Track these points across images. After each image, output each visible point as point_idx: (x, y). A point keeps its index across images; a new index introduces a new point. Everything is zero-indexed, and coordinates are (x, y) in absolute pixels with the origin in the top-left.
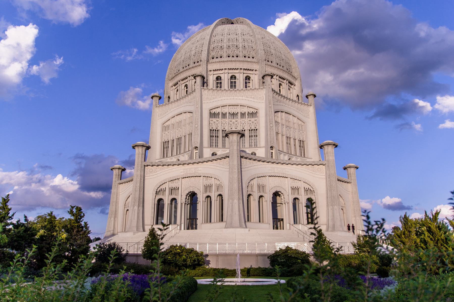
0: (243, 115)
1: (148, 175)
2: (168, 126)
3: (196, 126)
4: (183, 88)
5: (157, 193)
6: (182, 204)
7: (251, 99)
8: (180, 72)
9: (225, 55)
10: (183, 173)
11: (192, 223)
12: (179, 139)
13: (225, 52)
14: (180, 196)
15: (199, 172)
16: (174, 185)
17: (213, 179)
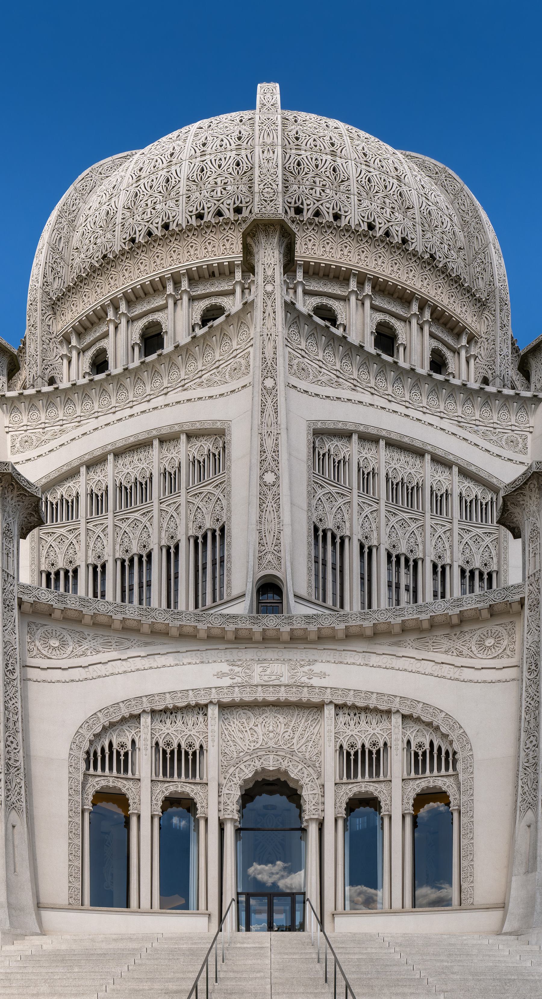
14: (213, 789)
15: (316, 682)
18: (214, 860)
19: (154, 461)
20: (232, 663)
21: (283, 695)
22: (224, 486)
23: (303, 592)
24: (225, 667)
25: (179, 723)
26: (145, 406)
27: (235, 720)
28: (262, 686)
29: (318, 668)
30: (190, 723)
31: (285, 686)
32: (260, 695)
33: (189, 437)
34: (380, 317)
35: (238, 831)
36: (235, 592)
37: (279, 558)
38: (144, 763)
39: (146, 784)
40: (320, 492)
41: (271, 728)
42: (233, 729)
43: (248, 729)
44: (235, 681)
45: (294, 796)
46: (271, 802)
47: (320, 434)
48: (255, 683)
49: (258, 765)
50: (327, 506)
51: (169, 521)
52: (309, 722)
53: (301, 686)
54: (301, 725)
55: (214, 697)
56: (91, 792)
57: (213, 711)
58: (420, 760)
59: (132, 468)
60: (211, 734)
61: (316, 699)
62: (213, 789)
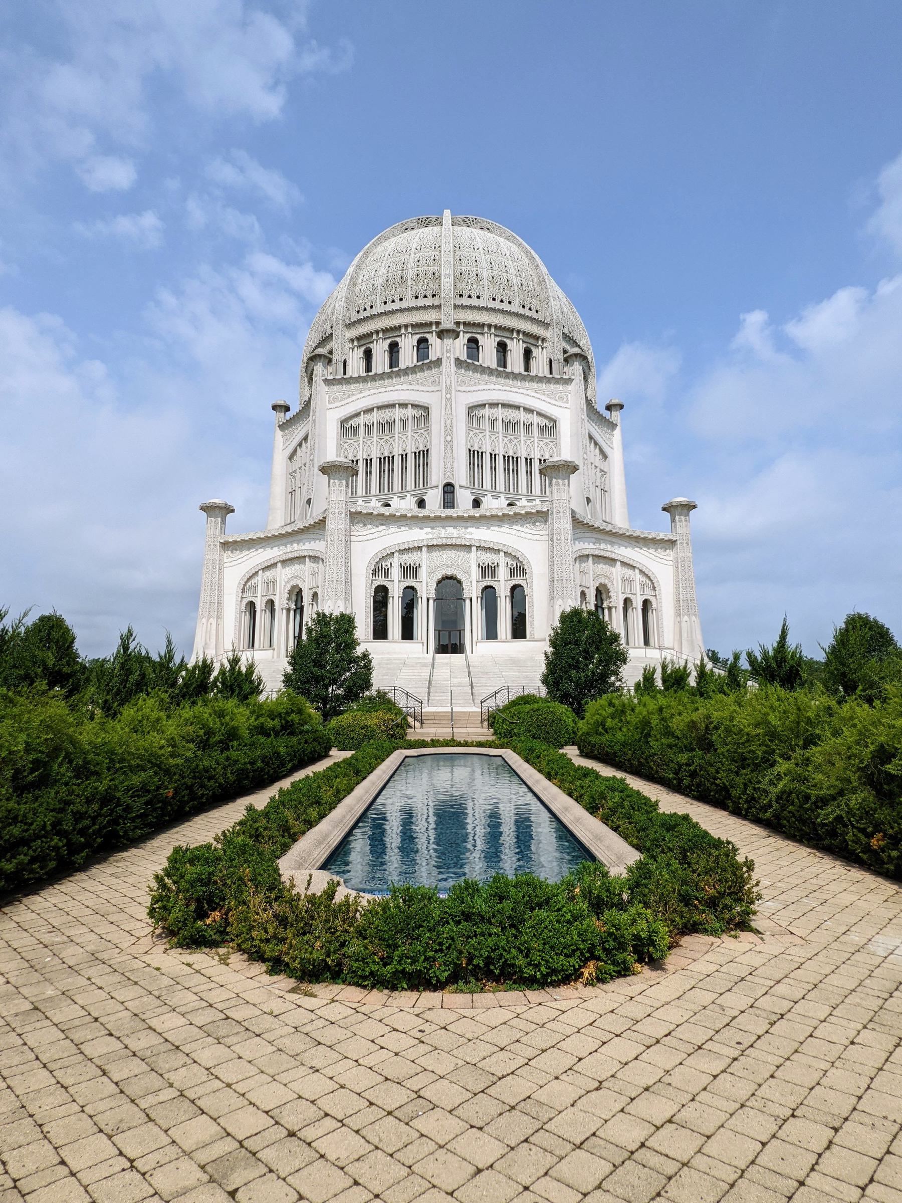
0: (528, 427)
1: (357, 533)
2: (355, 429)
3: (449, 438)
4: (387, 348)
5: (374, 573)
6: (428, 600)
7: (543, 397)
8: (374, 311)
9: (486, 295)
10: (430, 536)
11: (450, 643)
12: (386, 461)
13: (486, 288)
14: (424, 583)
15: (468, 536)
16: (410, 559)
17: (502, 554)
18: (425, 619)
19: (398, 413)
20: (433, 528)
21: (454, 542)
22: (428, 429)
23: (464, 484)
24: (429, 530)
26: (392, 388)
29: (470, 530)
32: (444, 542)
33: (412, 405)
34: (498, 339)
35: (434, 601)
36: (434, 484)
38: (396, 573)
39: (396, 581)
40: (471, 433)
45: (459, 582)
46: (449, 587)
47: (471, 409)
49: (444, 573)
50: (475, 439)
51: (404, 442)
53: (462, 538)
56: (374, 587)
57: (425, 549)
58: (512, 573)
60: (423, 559)
62: (424, 583)
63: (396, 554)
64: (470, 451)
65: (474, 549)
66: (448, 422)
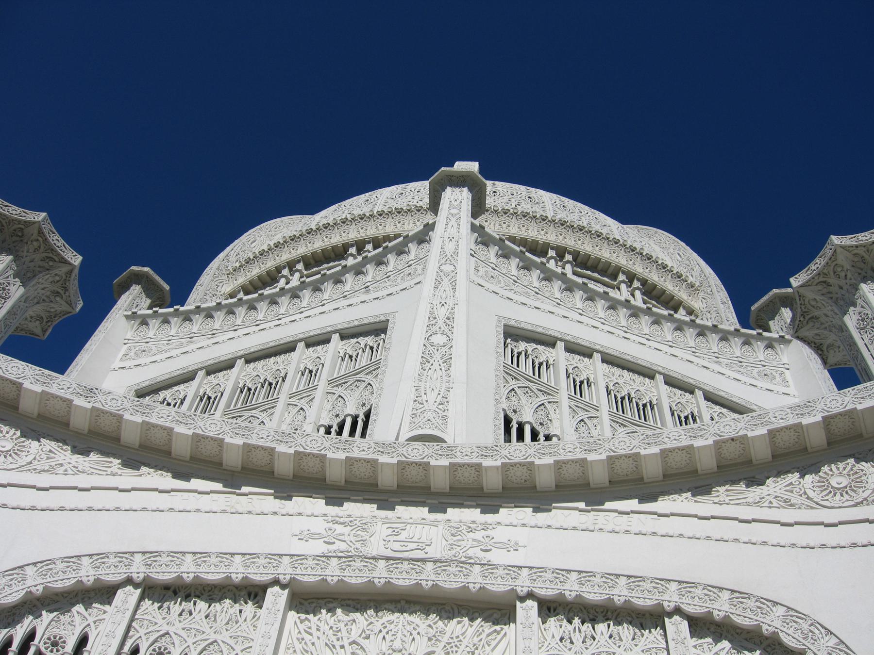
15: (497, 557)
25: (199, 616)
27: (321, 625)
28: (388, 559)
30: (222, 618)
31: (436, 562)
37: (445, 418)
41: (397, 644)
42: (315, 640)
43: (346, 642)
44: (332, 547)
48: (374, 554)
52: (484, 636)
53: (467, 563)
54: (465, 642)
55: (285, 571)
57: (276, 598)
59: (265, 369)
61: (498, 585)
63: (127, 597)
64: (507, 421)
65: (527, 611)
66: (442, 312)
